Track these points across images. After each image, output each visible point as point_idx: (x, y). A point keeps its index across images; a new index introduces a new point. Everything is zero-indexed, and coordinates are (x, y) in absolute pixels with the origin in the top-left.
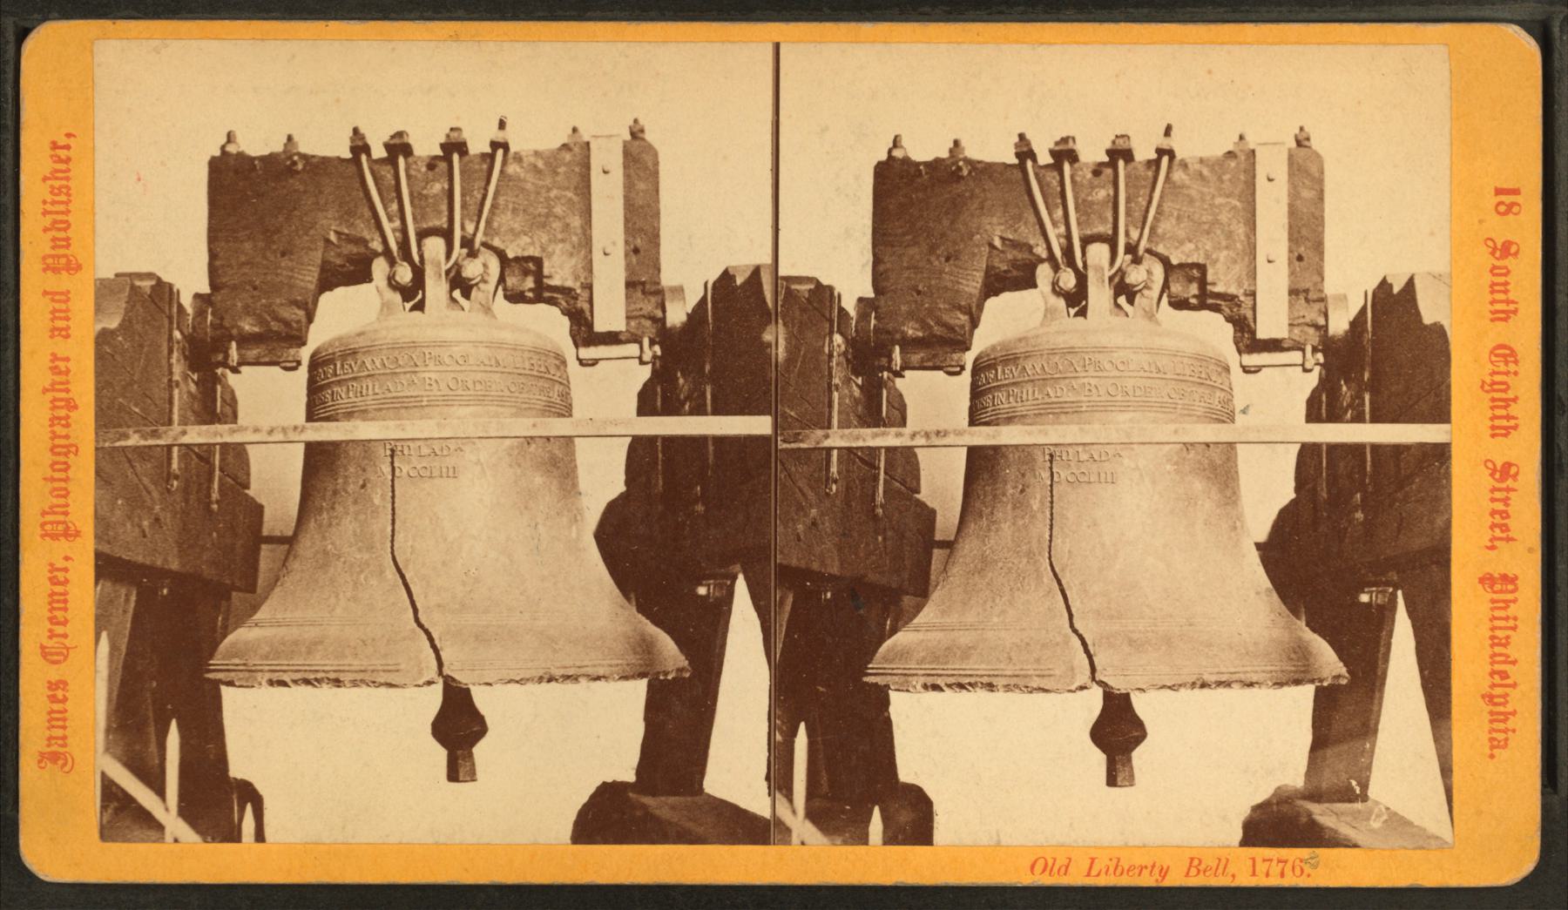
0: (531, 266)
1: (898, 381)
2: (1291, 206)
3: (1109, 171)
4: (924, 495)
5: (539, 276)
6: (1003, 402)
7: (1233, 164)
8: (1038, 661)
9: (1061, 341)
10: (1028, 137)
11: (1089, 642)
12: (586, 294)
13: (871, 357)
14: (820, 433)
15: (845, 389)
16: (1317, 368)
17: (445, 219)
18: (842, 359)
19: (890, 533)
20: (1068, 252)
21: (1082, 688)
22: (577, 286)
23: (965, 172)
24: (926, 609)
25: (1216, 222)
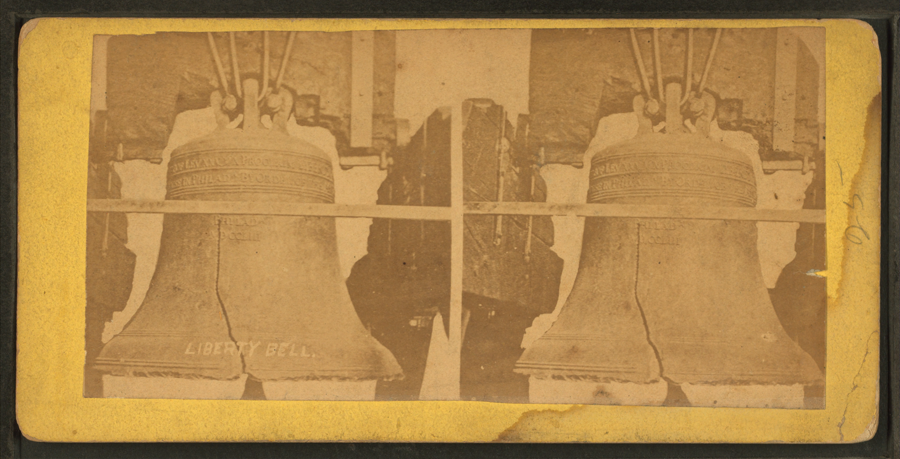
0: (313, 101)
5: (317, 108)
11: (659, 351)
12: (346, 122)
15: (509, 174)
17: (258, 68)
18: (507, 155)
19: (533, 272)
20: (654, 88)
21: (654, 381)
22: (341, 115)
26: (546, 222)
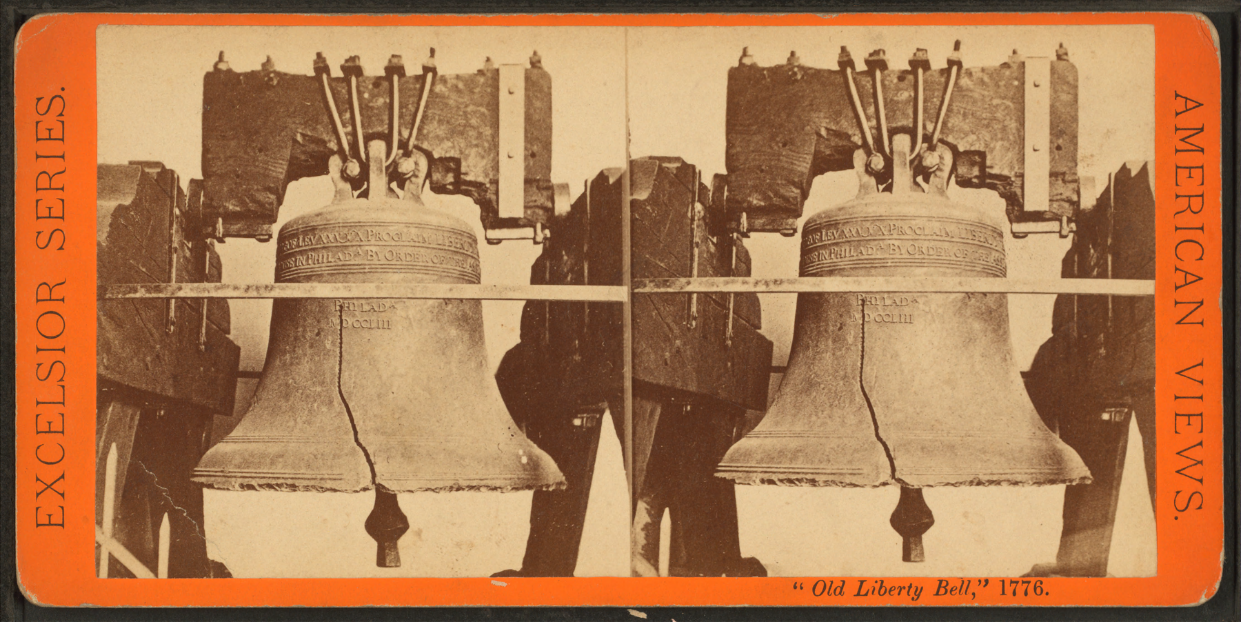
1: (745, 241)
2: (1052, 106)
3: (911, 77)
4: (765, 330)
6: (826, 258)
7: (1008, 73)
8: (850, 462)
9: (872, 211)
10: (848, 49)
13: (724, 221)
14: (683, 280)
15: (703, 245)
16: (1071, 235)
20: (878, 140)
21: (884, 484)
23: (799, 77)
24: (764, 421)
25: (995, 119)
26: (749, 302)
